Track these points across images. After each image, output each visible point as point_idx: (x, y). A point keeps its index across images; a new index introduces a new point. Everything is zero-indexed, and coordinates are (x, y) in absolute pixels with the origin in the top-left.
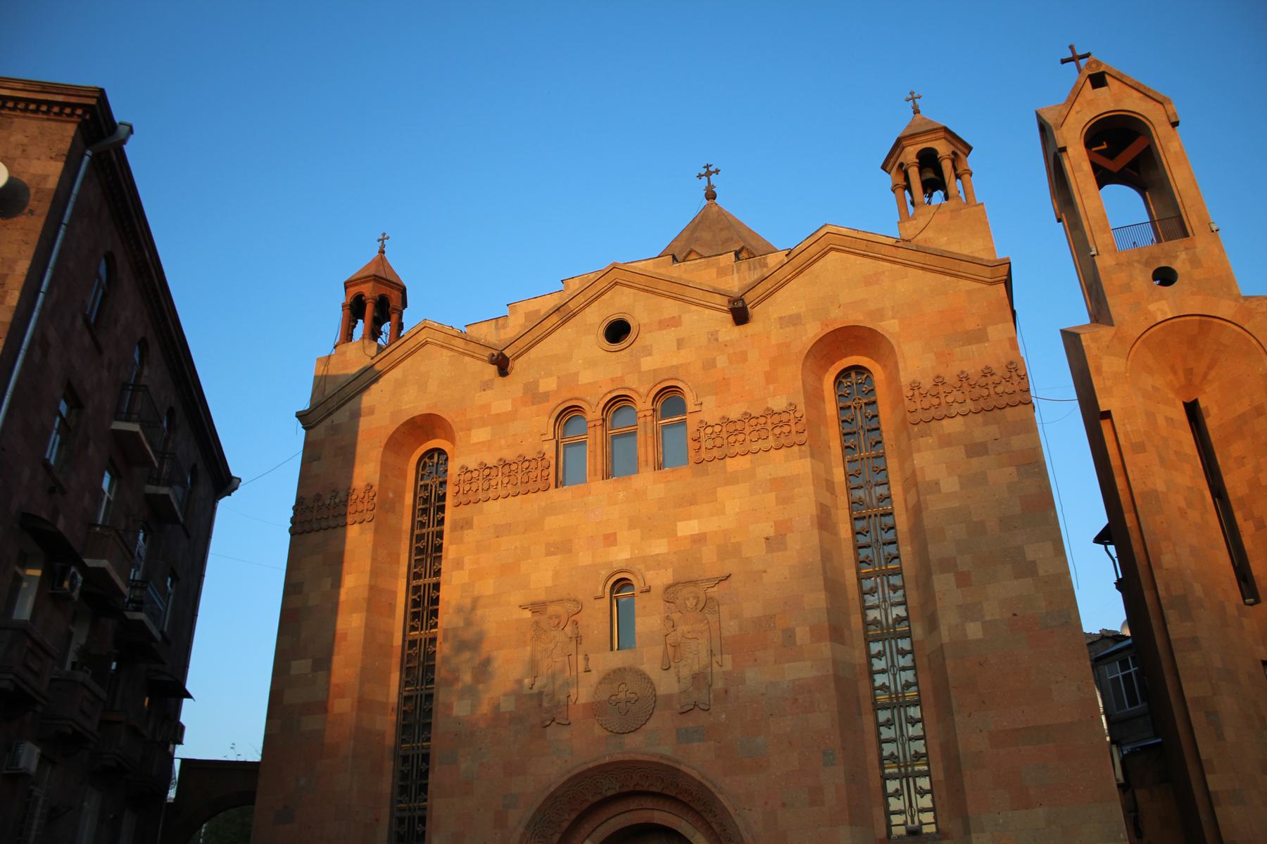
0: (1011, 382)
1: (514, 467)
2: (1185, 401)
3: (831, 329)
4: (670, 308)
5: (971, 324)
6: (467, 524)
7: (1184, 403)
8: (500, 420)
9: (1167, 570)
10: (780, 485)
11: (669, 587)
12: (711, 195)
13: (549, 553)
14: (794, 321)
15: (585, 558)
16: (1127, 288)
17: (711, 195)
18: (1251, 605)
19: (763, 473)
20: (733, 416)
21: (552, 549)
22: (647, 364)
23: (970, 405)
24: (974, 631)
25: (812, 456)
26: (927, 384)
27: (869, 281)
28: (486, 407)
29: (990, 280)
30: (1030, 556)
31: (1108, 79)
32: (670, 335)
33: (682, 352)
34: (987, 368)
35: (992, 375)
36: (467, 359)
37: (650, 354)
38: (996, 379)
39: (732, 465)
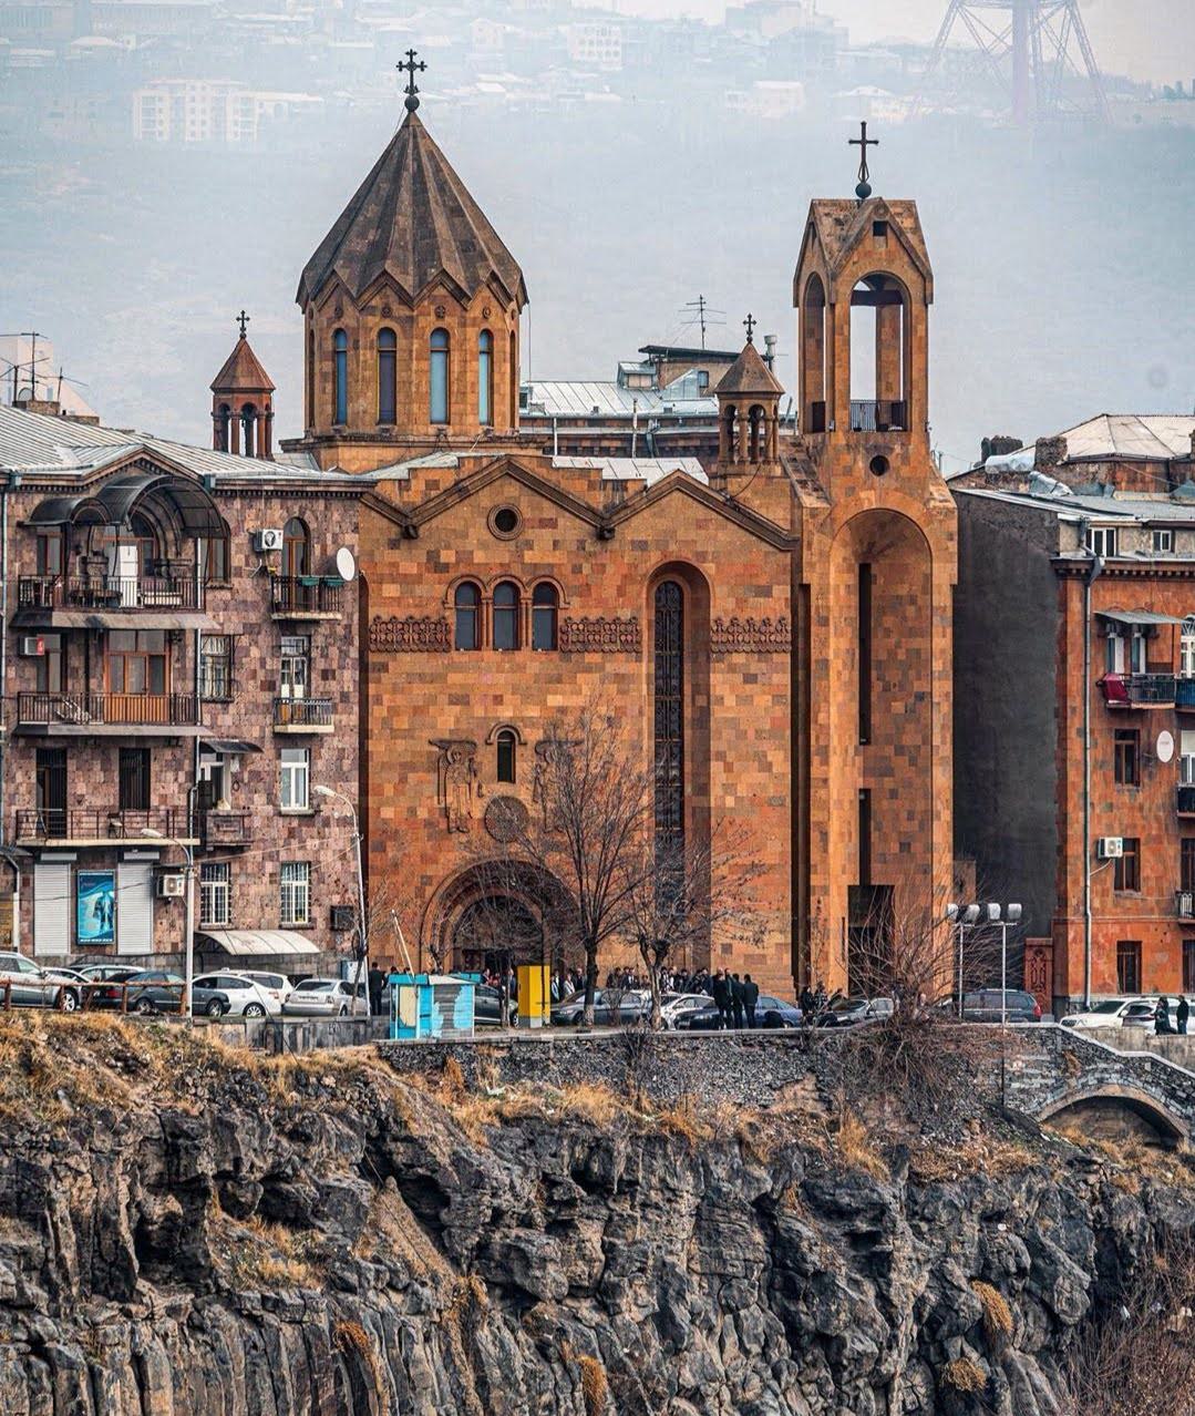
1: (423, 627)
3: (667, 560)
4: (549, 510)
5: (763, 581)
6: (384, 668)
8: (405, 580)
10: (620, 678)
11: (539, 743)
12: (412, 105)
13: (451, 703)
14: (642, 546)
15: (479, 712)
16: (848, 471)
19: (609, 667)
20: (592, 618)
21: (454, 700)
22: (529, 556)
23: (753, 647)
24: (730, 802)
26: (727, 623)
27: (700, 525)
28: (394, 565)
30: (770, 759)
31: (889, 231)
32: (547, 535)
33: (557, 553)
36: (373, 514)
37: (531, 549)
39: (592, 658)
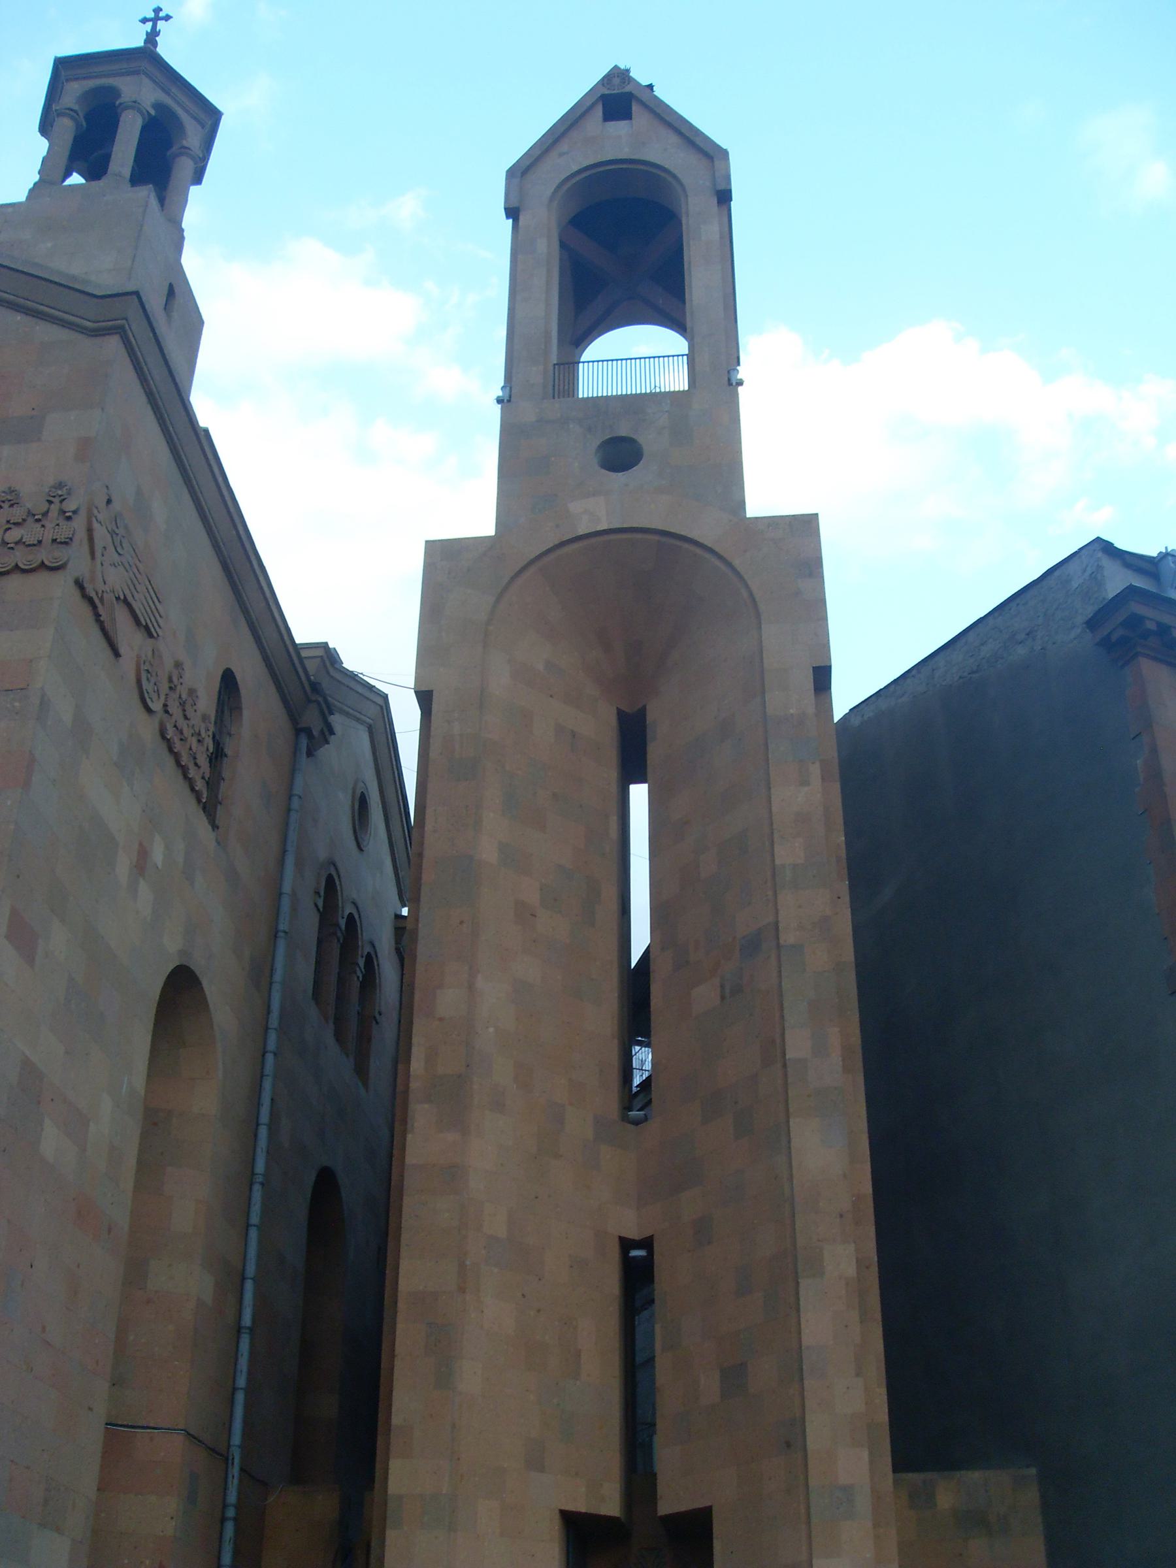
0: (43, 523)
2: (624, 708)
7: (621, 715)
9: (441, 1019)
18: (637, 1122)
29: (88, 324)
31: (635, 108)
34: (11, 491)
35: (12, 506)
38: (17, 514)
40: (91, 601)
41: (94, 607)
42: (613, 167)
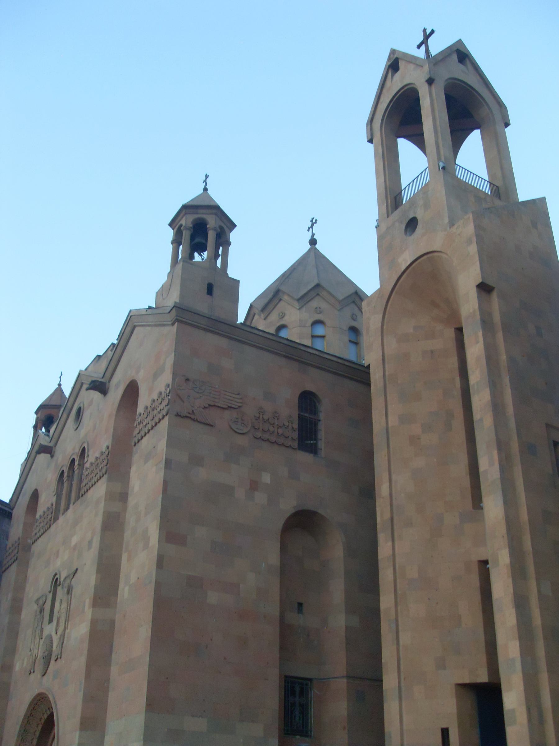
12: (313, 242)
14: (117, 386)
17: (313, 242)
25: (109, 480)
40: (186, 417)
41: (190, 418)
42: (398, 94)
